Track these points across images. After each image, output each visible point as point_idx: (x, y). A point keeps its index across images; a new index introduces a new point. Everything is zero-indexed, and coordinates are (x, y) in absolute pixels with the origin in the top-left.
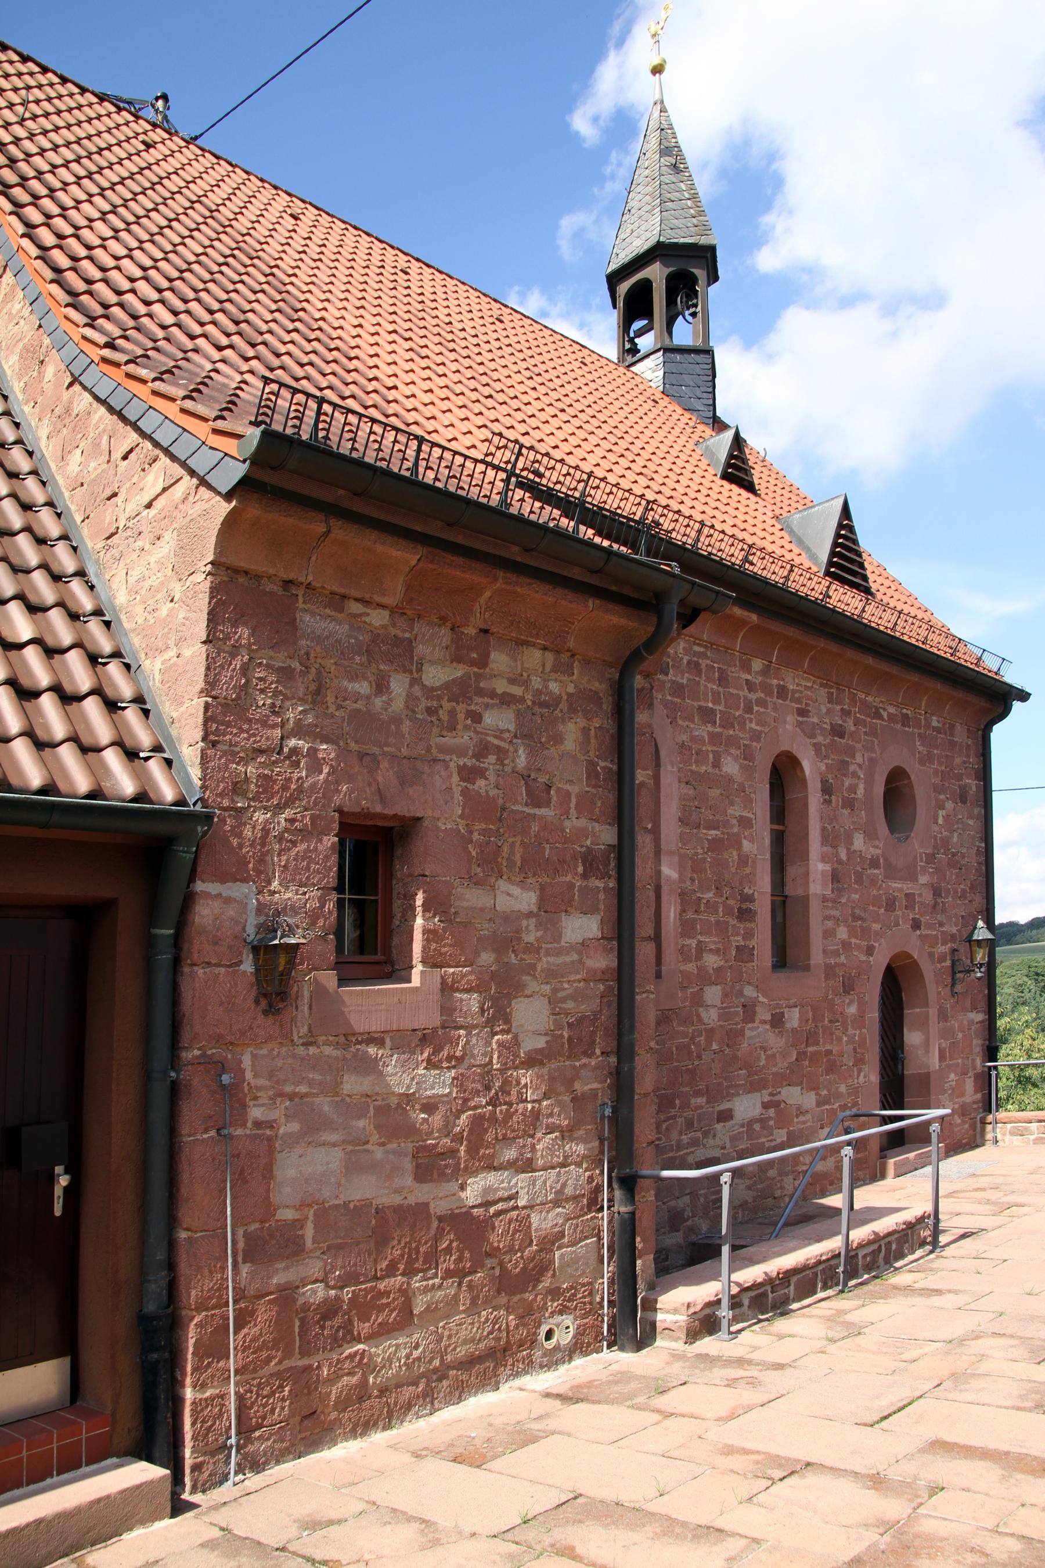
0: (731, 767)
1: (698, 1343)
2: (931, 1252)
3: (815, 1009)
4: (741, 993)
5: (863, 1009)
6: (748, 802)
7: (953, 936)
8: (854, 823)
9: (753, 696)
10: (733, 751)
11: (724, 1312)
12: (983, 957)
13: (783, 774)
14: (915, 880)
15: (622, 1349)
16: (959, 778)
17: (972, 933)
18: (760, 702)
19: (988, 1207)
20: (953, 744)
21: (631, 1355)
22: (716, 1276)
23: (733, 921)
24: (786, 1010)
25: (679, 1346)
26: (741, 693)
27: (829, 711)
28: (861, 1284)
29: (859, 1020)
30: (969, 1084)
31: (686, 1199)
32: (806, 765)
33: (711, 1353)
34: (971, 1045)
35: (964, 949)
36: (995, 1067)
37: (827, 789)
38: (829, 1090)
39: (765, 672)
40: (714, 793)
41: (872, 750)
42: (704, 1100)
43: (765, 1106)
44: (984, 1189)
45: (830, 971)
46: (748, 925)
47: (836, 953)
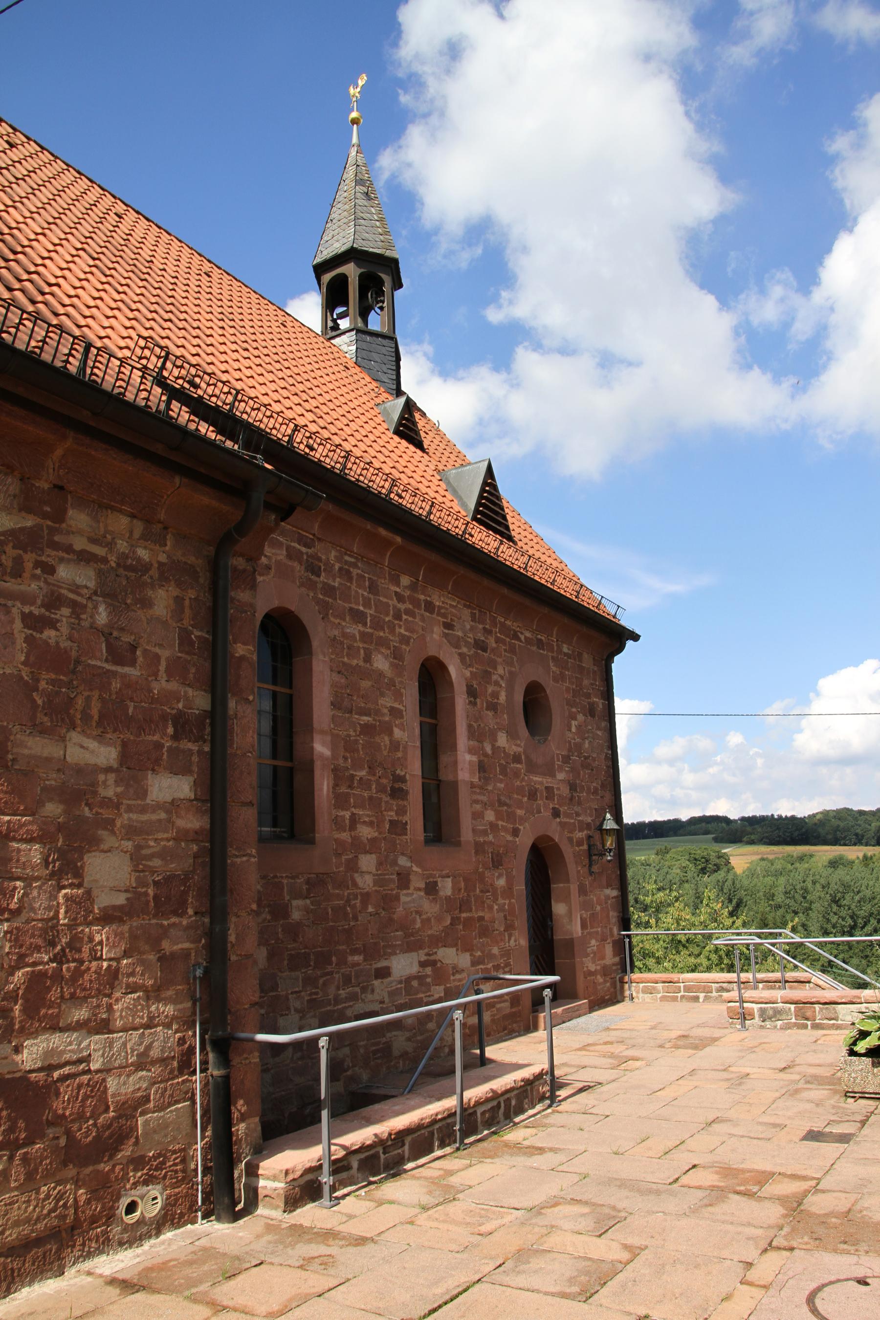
0: (381, 663)
1: (299, 1211)
2: (550, 1106)
3: (466, 880)
4: (395, 863)
5: (510, 883)
6: (398, 696)
7: (588, 825)
8: (497, 723)
9: (402, 607)
10: (383, 650)
11: (326, 1179)
12: (611, 844)
13: (431, 676)
14: (553, 776)
15: (218, 1219)
16: (588, 696)
17: (602, 824)
18: (408, 612)
19: (610, 1061)
20: (581, 669)
21: (226, 1225)
22: (317, 1141)
23: (385, 798)
24: (439, 880)
25: (277, 1214)
26: (390, 602)
27: (472, 629)
28: (479, 1140)
29: (508, 891)
30: (609, 950)
31: (346, 1050)
32: (453, 670)
33: (305, 1224)
34: (608, 916)
35: (597, 836)
36: (629, 936)
37: (472, 693)
38: (483, 952)
39: (413, 587)
40: (366, 684)
41: (511, 664)
42: (361, 957)
43: (423, 964)
44: (611, 1043)
45: (479, 848)
46: (401, 802)
47: (485, 833)
